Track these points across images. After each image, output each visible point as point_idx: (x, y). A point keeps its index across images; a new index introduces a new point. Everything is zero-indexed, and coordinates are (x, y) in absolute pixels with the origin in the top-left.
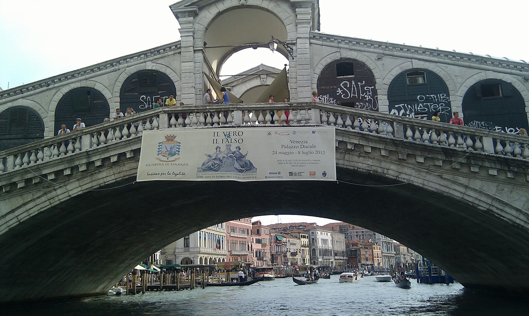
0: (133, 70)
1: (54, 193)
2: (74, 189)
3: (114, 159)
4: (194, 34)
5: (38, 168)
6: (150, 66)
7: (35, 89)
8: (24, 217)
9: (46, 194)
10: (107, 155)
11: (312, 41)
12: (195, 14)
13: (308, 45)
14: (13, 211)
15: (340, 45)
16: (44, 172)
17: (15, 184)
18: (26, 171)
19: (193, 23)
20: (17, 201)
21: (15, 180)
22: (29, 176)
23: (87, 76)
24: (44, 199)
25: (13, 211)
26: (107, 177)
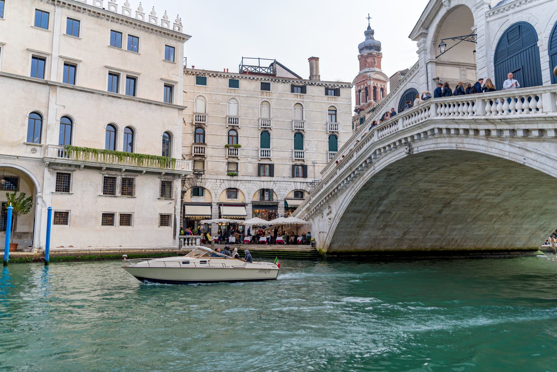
0: (402, 93)
4: (426, 50)
11: (489, 19)
12: (425, 35)
13: (483, 27)
15: (509, 13)
19: (425, 42)
26: (368, 175)
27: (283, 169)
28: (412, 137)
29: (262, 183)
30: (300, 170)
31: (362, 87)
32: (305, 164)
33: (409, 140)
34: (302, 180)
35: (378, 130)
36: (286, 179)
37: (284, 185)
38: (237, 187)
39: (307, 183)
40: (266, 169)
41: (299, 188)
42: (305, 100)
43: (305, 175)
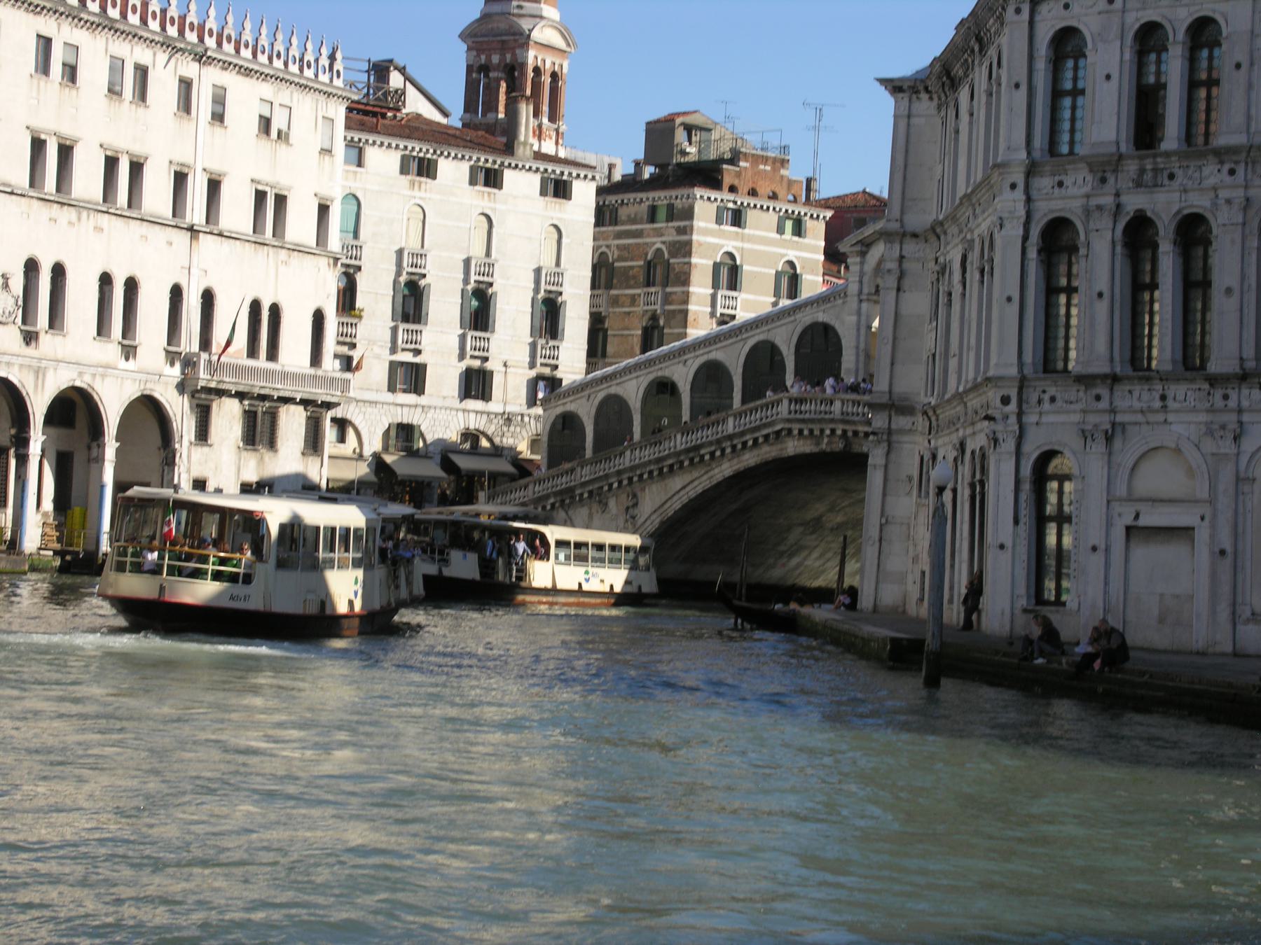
1: (712, 473)
2: (725, 469)
3: (750, 443)
5: (696, 448)
6: (821, 317)
7: (726, 339)
8: (692, 494)
9: (707, 472)
10: (744, 439)
12: (863, 254)
14: (684, 488)
16: (702, 452)
17: (682, 463)
18: (688, 451)
20: (687, 478)
21: (682, 458)
22: (691, 455)
23: (769, 327)
24: (705, 477)
25: (684, 488)
26: (750, 459)
27: (444, 374)
28: (856, 433)
29: (399, 409)
30: (476, 384)
31: (495, 59)
32: (489, 366)
33: (850, 434)
34: (477, 405)
35: (790, 401)
36: (448, 403)
37: (442, 415)
38: (349, 417)
39: (488, 414)
40: (411, 377)
41: (472, 427)
42: (498, 206)
43: (485, 395)
